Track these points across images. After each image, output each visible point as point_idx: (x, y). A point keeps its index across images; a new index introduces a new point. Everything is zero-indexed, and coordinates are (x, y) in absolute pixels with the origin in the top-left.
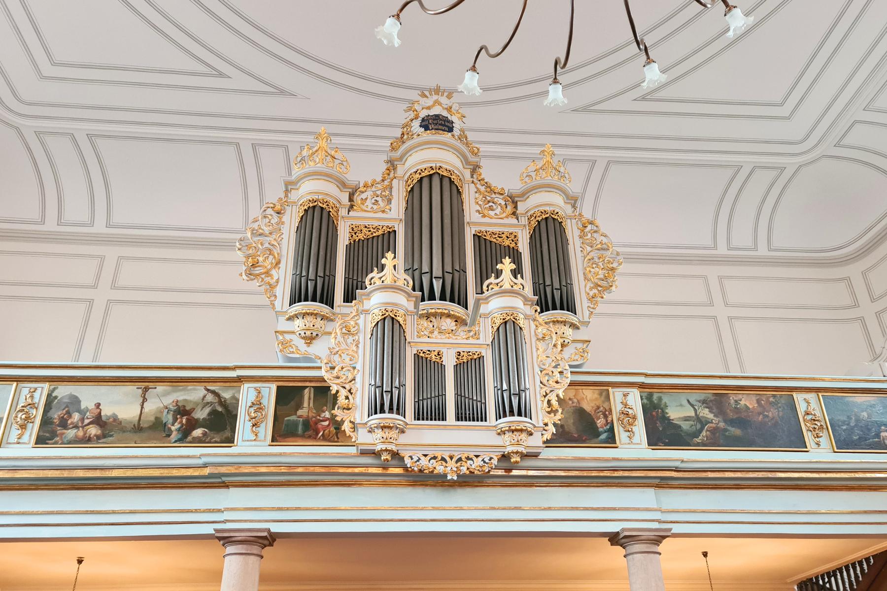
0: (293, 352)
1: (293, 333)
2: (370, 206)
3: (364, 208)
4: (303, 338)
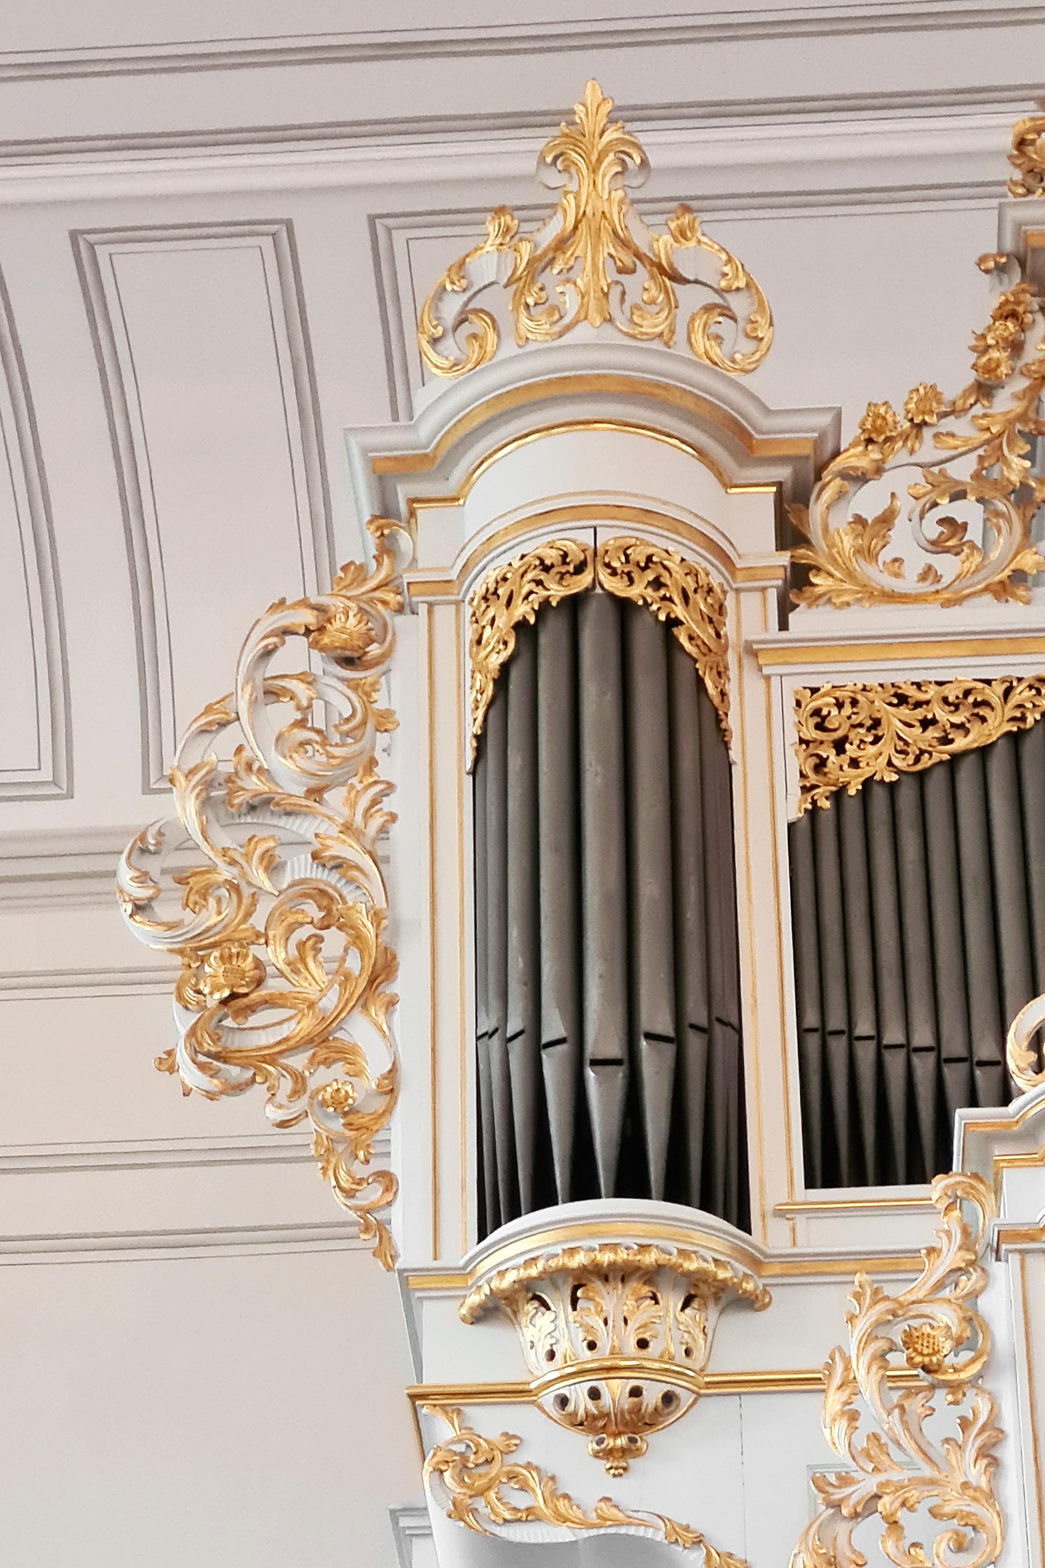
0: (531, 1515)
1: (517, 1393)
2: (913, 568)
3: (878, 576)
4: (585, 1424)
